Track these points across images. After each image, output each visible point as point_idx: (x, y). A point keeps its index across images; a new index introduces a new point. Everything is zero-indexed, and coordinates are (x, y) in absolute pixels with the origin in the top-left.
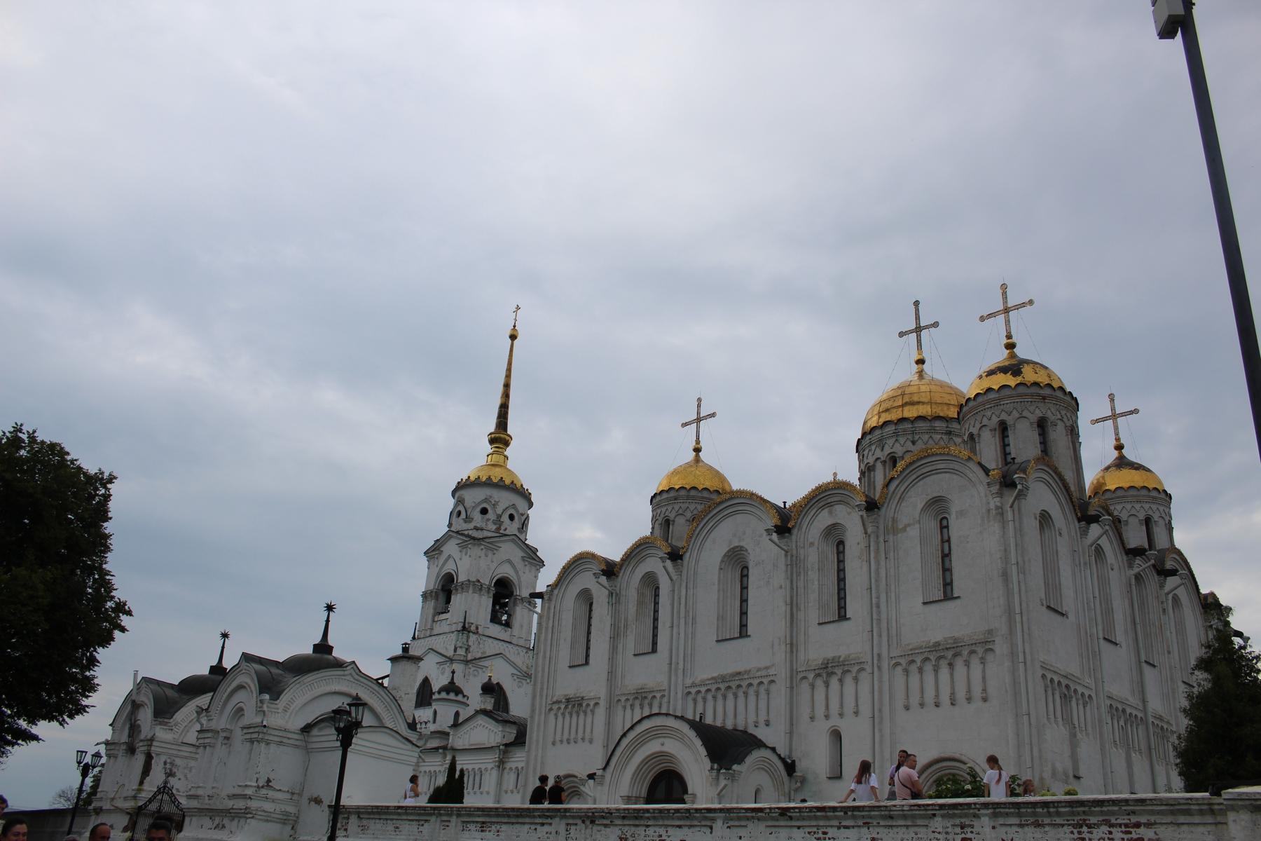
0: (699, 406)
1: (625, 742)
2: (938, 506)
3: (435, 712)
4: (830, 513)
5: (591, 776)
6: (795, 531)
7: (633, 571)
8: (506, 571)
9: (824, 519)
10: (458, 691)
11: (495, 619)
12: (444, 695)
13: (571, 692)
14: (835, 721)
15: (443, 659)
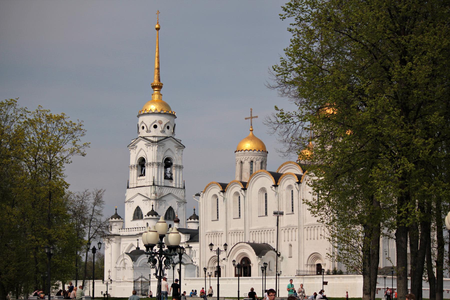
0: (251, 112)
1: (233, 250)
3: (147, 224)
5: (224, 259)
6: (279, 186)
7: (231, 190)
8: (169, 154)
10: (156, 214)
11: (166, 178)
12: (150, 216)
14: (290, 242)
15: (145, 199)
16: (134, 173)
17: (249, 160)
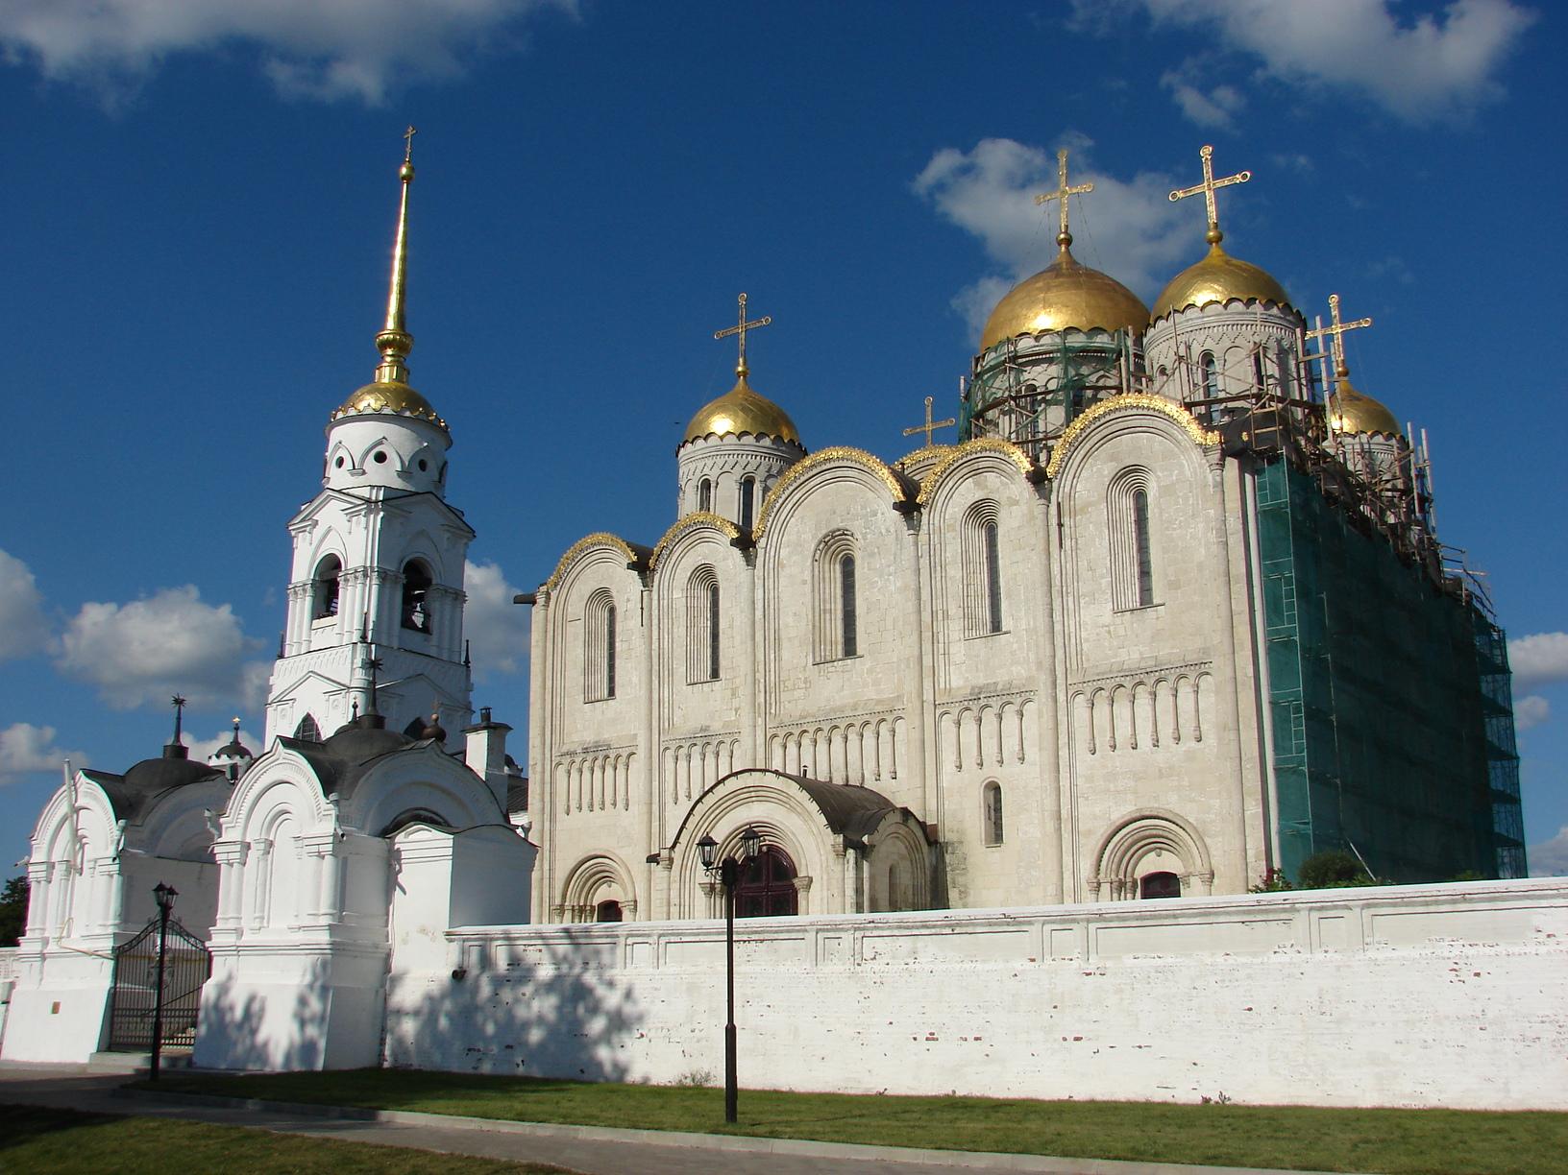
2: (1131, 478)
4: (976, 484)
8: (421, 550)
9: (967, 492)
11: (407, 623)
13: (589, 737)
16: (300, 607)
17: (738, 472)
